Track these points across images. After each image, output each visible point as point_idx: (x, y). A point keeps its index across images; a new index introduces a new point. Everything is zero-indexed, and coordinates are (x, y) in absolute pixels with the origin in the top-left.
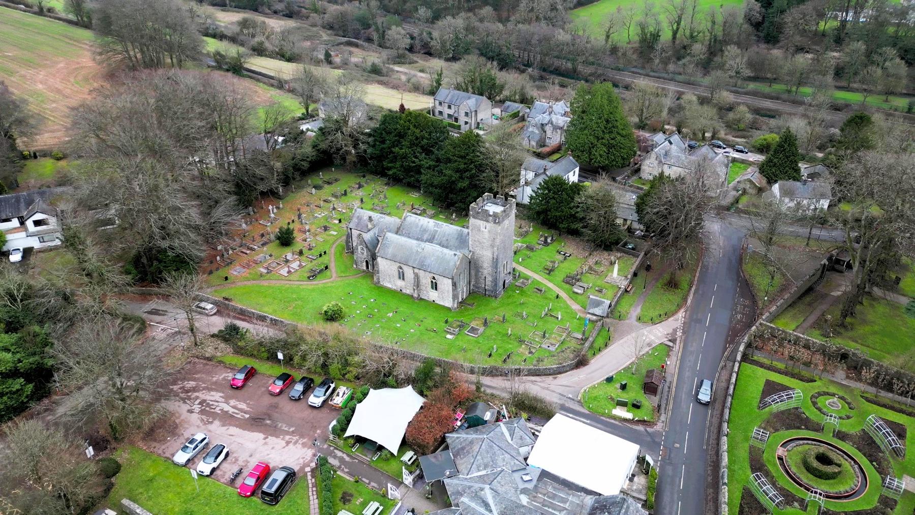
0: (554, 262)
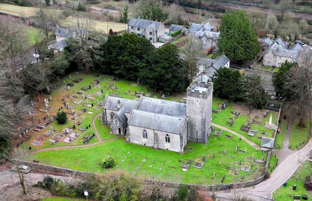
0: (231, 119)
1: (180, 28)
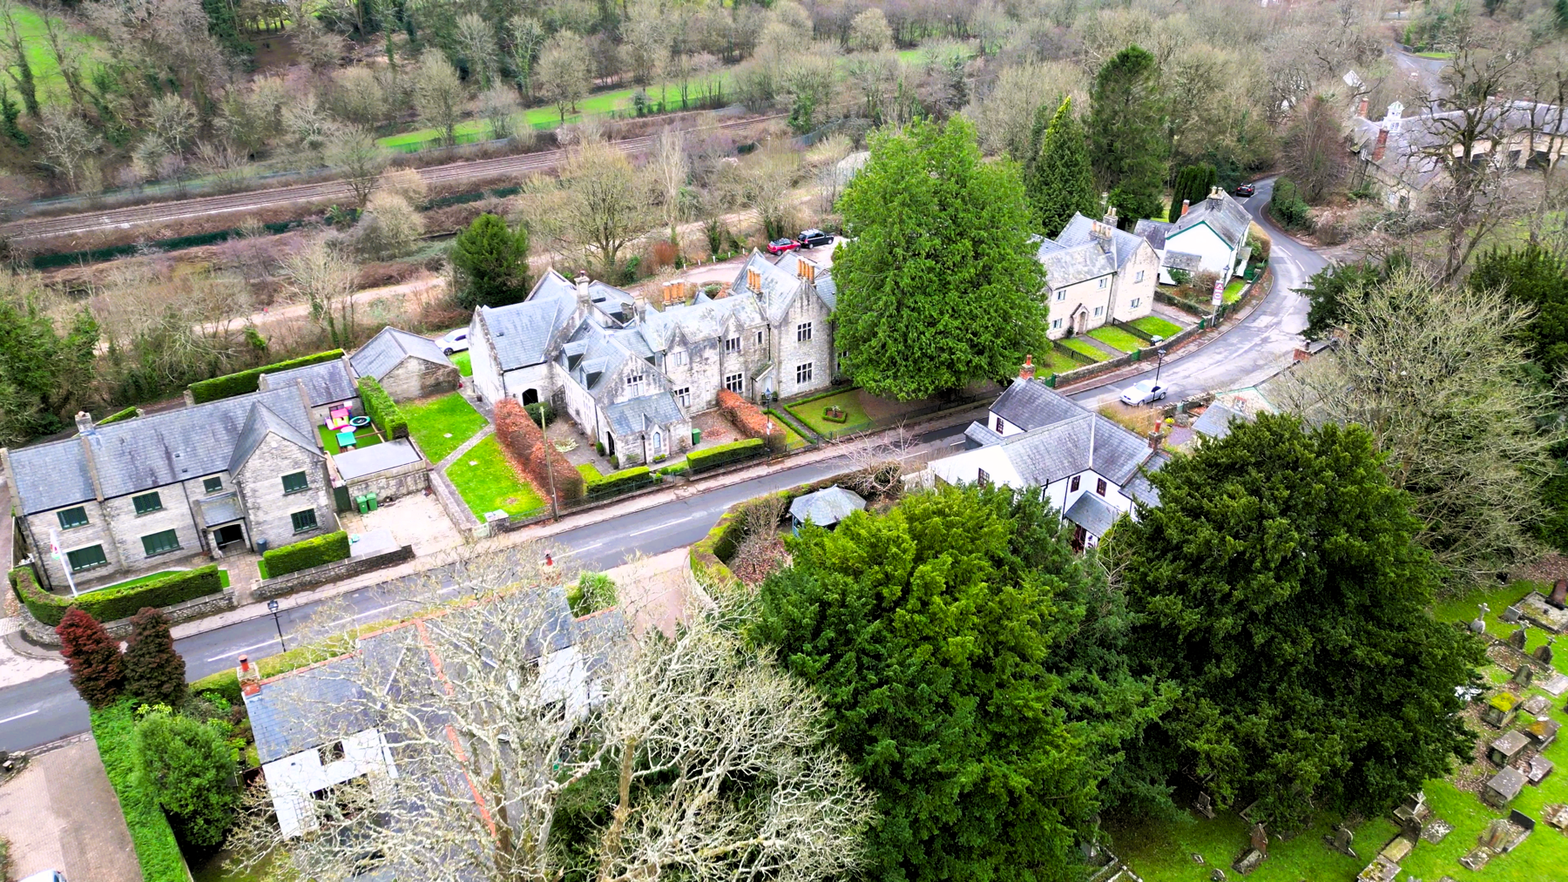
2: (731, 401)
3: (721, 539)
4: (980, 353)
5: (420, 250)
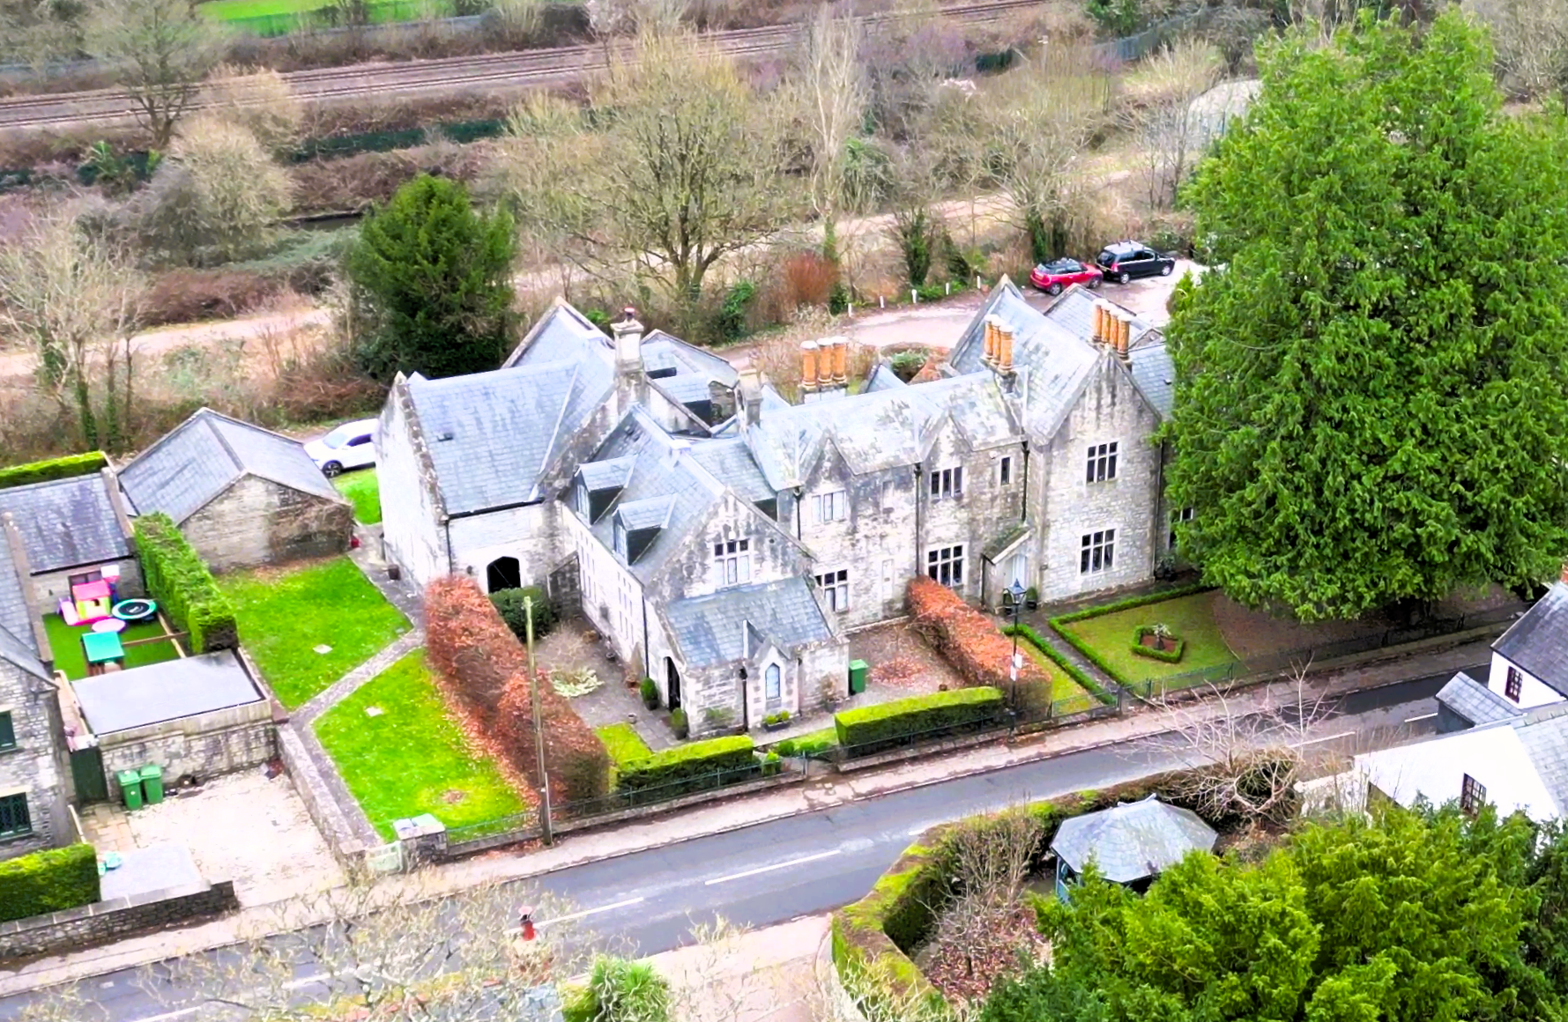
1: (81, 510)
2: (936, 604)
3: (901, 900)
4: (1479, 525)
5: (282, 247)
